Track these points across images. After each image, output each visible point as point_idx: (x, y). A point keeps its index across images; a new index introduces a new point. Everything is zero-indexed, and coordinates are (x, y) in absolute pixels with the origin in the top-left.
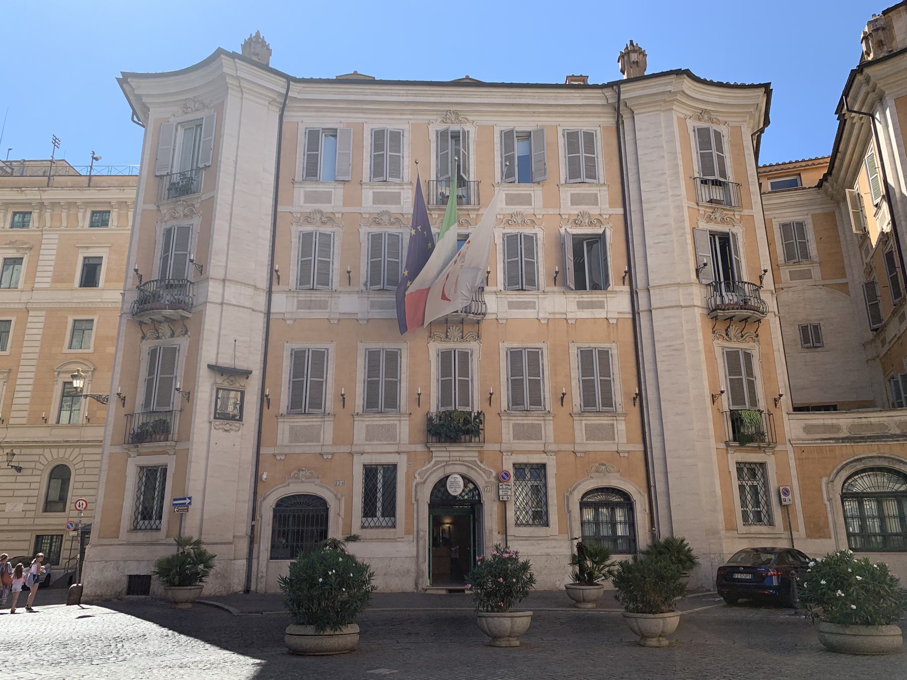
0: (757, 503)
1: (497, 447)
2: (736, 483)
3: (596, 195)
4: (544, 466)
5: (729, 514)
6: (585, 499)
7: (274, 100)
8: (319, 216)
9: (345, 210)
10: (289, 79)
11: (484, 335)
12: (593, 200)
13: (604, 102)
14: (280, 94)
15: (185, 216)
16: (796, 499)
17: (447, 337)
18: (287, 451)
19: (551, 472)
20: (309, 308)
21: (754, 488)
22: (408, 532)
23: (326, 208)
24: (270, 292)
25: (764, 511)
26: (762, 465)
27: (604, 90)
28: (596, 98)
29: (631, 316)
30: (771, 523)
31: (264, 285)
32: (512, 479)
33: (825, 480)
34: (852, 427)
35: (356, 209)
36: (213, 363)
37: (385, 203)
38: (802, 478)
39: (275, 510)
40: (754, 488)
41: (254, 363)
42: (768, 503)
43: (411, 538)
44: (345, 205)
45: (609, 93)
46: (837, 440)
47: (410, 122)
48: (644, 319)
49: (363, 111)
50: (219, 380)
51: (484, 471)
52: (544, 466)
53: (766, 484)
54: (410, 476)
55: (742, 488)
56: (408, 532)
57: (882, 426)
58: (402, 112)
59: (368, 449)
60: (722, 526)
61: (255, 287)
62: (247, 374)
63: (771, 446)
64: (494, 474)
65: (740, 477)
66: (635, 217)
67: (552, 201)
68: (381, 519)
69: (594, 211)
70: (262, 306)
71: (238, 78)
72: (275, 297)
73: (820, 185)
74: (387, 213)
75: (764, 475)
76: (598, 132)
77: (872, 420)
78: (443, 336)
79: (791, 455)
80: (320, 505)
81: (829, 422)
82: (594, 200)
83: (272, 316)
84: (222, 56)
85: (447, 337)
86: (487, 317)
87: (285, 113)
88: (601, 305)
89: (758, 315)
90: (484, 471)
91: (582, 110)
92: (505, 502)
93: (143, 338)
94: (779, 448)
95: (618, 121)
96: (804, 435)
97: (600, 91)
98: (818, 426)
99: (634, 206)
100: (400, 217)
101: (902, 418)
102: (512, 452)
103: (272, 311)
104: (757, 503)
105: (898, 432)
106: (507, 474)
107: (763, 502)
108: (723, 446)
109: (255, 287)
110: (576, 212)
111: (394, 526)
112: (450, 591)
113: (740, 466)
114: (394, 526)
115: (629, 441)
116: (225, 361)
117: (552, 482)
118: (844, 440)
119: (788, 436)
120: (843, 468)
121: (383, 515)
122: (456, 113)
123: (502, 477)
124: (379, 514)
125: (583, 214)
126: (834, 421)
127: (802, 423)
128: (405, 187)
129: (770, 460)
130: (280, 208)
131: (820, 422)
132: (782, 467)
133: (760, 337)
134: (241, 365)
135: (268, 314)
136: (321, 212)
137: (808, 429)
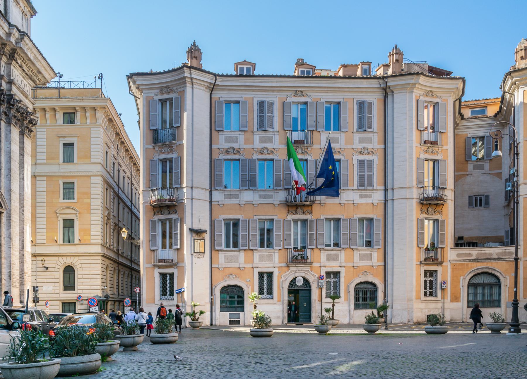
0: (431, 288)
1: (318, 264)
2: (423, 279)
3: (371, 138)
4: (339, 272)
5: (418, 292)
6: (358, 287)
7: (208, 86)
8: (232, 151)
9: (245, 147)
10: (215, 75)
11: (314, 212)
12: (370, 141)
13: (378, 86)
14: (211, 84)
15: (169, 152)
16: (449, 286)
17: (296, 212)
18: (224, 266)
19: (342, 275)
20: (230, 199)
21: (431, 282)
22: (279, 301)
23: (235, 146)
24: (211, 191)
25: (434, 291)
26: (436, 271)
27: (379, 80)
28: (375, 84)
29: (384, 202)
30: (436, 296)
31: (208, 187)
32: (325, 278)
33: (462, 278)
34: (478, 254)
35: (251, 146)
36: (190, 227)
37: (265, 142)
38: (453, 277)
39: (220, 292)
40: (431, 282)
41: (206, 226)
42: (436, 288)
43: (280, 303)
44: (245, 144)
45: (381, 81)
46: (470, 260)
47: (278, 96)
48: (390, 203)
49: (253, 91)
50: (194, 235)
51: (313, 275)
52: (339, 272)
53: (436, 280)
54: (280, 277)
55: (425, 281)
56: (279, 301)
57: (491, 254)
58: (273, 91)
59: (260, 265)
60: (414, 297)
61: (205, 189)
62: (206, 231)
63: (441, 264)
64: (317, 276)
65: (425, 276)
66: (389, 151)
67: (350, 141)
68: (267, 295)
69: (369, 146)
70: (208, 199)
71: (192, 79)
72: (213, 193)
73: (496, 116)
74: (266, 148)
75: (436, 276)
76: (375, 102)
77: (487, 252)
78: (294, 212)
79: (449, 267)
80: (240, 289)
81: (468, 252)
82: (370, 141)
83: (213, 203)
84: (185, 68)
85: (296, 212)
86: (316, 202)
87: (213, 92)
88: (370, 196)
89: (442, 202)
90: (313, 275)
91: (367, 90)
92: (321, 288)
93: (154, 214)
94: (444, 264)
95: (385, 96)
96: (456, 258)
97: (377, 80)
98: (463, 254)
99: (389, 145)
100: (273, 150)
101: (499, 251)
102: (325, 267)
103: (213, 200)
104: (431, 288)
105: (496, 257)
106: (323, 276)
107: (434, 287)
108: (419, 263)
109: (205, 189)
110: (361, 147)
111: (272, 298)
112: (297, 324)
113: (426, 272)
114: (272, 298)
115: (378, 261)
116: (196, 227)
117: (342, 279)
118: (473, 260)
119: (449, 259)
120: (470, 273)
121: (268, 294)
122: (301, 92)
123: (321, 278)
124: (265, 293)
125: (365, 149)
126: (470, 252)
127: (456, 253)
128: (275, 133)
129: (439, 269)
130: (213, 146)
131: (464, 252)
132: (445, 273)
133: (443, 213)
134: (203, 228)
135: (211, 202)
136: (233, 148)
137: (458, 255)
